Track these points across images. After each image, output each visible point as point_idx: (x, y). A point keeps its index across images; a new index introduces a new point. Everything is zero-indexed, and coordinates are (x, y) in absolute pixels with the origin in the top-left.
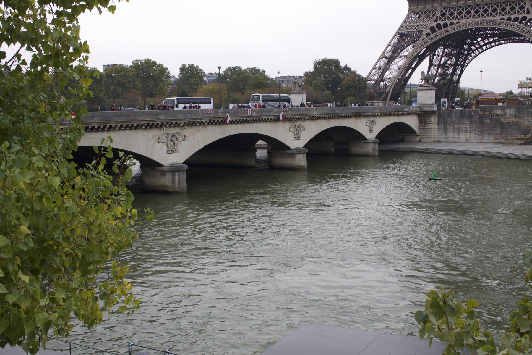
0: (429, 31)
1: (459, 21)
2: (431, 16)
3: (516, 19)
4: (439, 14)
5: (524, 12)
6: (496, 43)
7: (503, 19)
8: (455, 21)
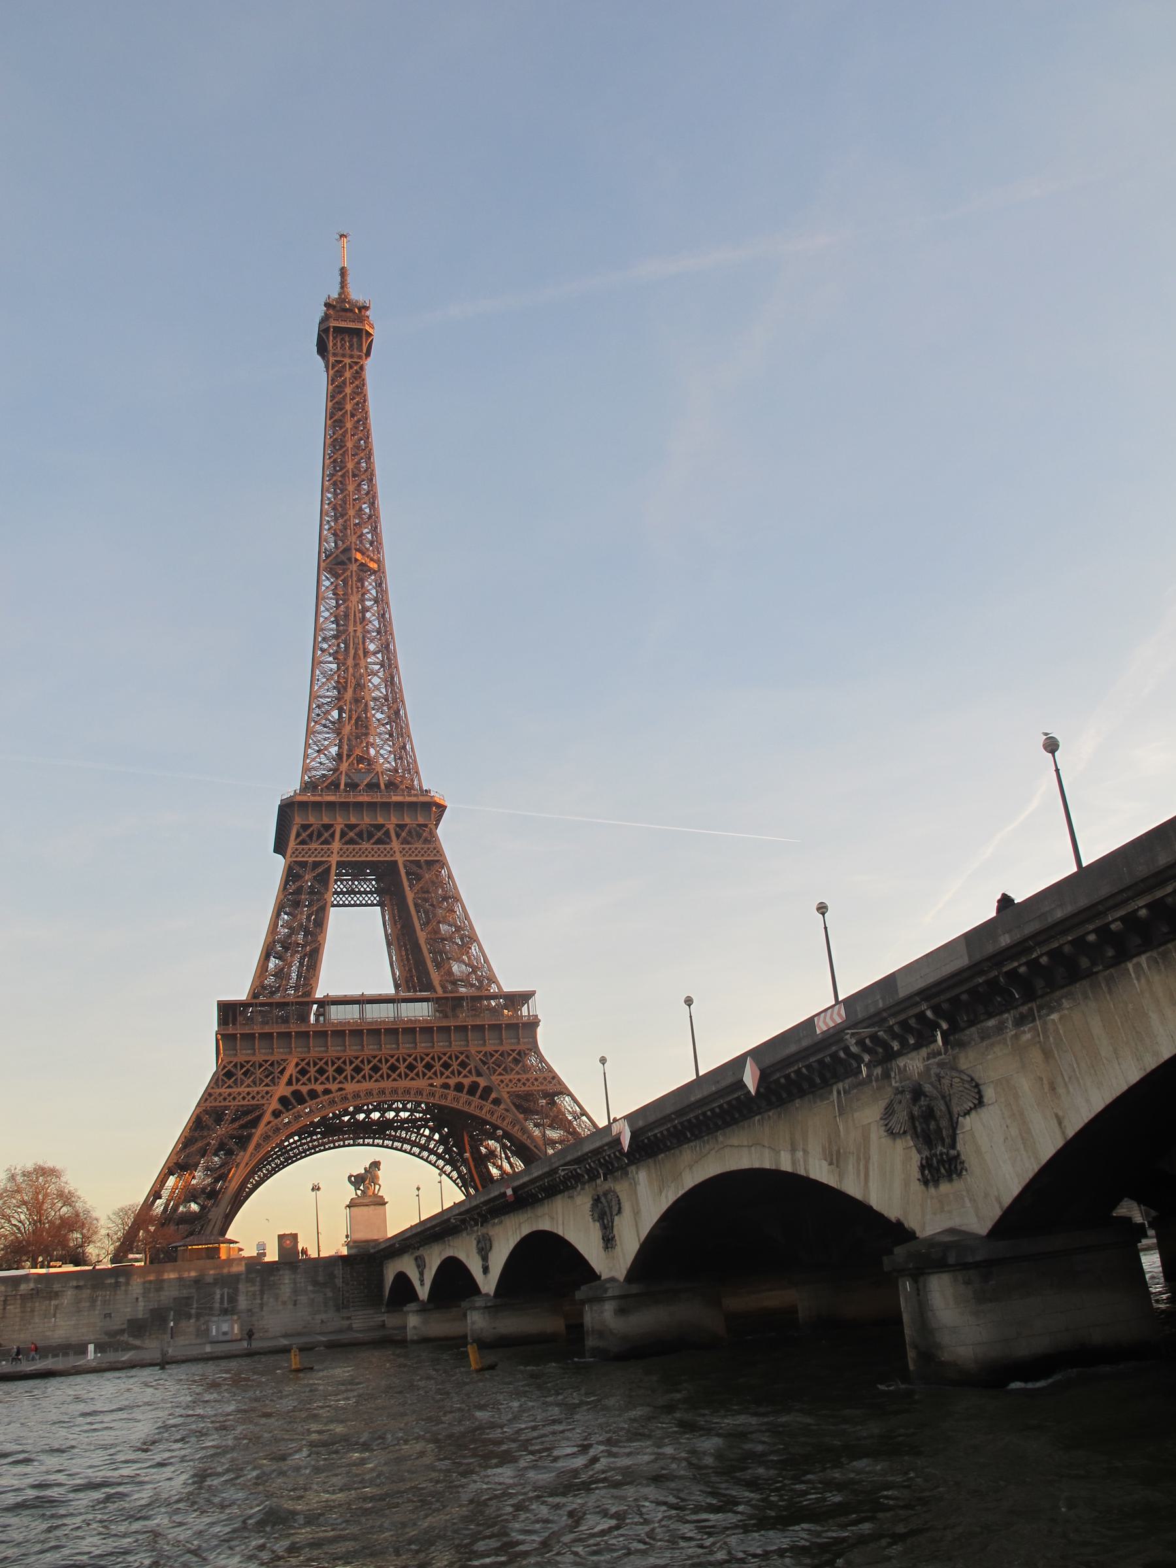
0: (280, 1107)
1: (340, 1086)
2: (276, 1074)
3: (459, 1087)
4: (291, 1070)
5: (470, 1072)
6: (396, 1144)
7: (431, 1085)
8: (334, 1087)
